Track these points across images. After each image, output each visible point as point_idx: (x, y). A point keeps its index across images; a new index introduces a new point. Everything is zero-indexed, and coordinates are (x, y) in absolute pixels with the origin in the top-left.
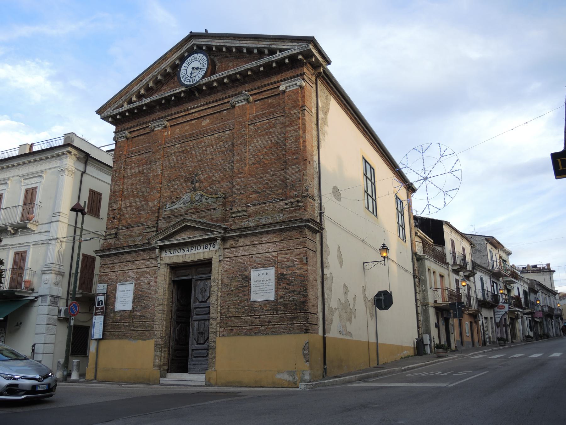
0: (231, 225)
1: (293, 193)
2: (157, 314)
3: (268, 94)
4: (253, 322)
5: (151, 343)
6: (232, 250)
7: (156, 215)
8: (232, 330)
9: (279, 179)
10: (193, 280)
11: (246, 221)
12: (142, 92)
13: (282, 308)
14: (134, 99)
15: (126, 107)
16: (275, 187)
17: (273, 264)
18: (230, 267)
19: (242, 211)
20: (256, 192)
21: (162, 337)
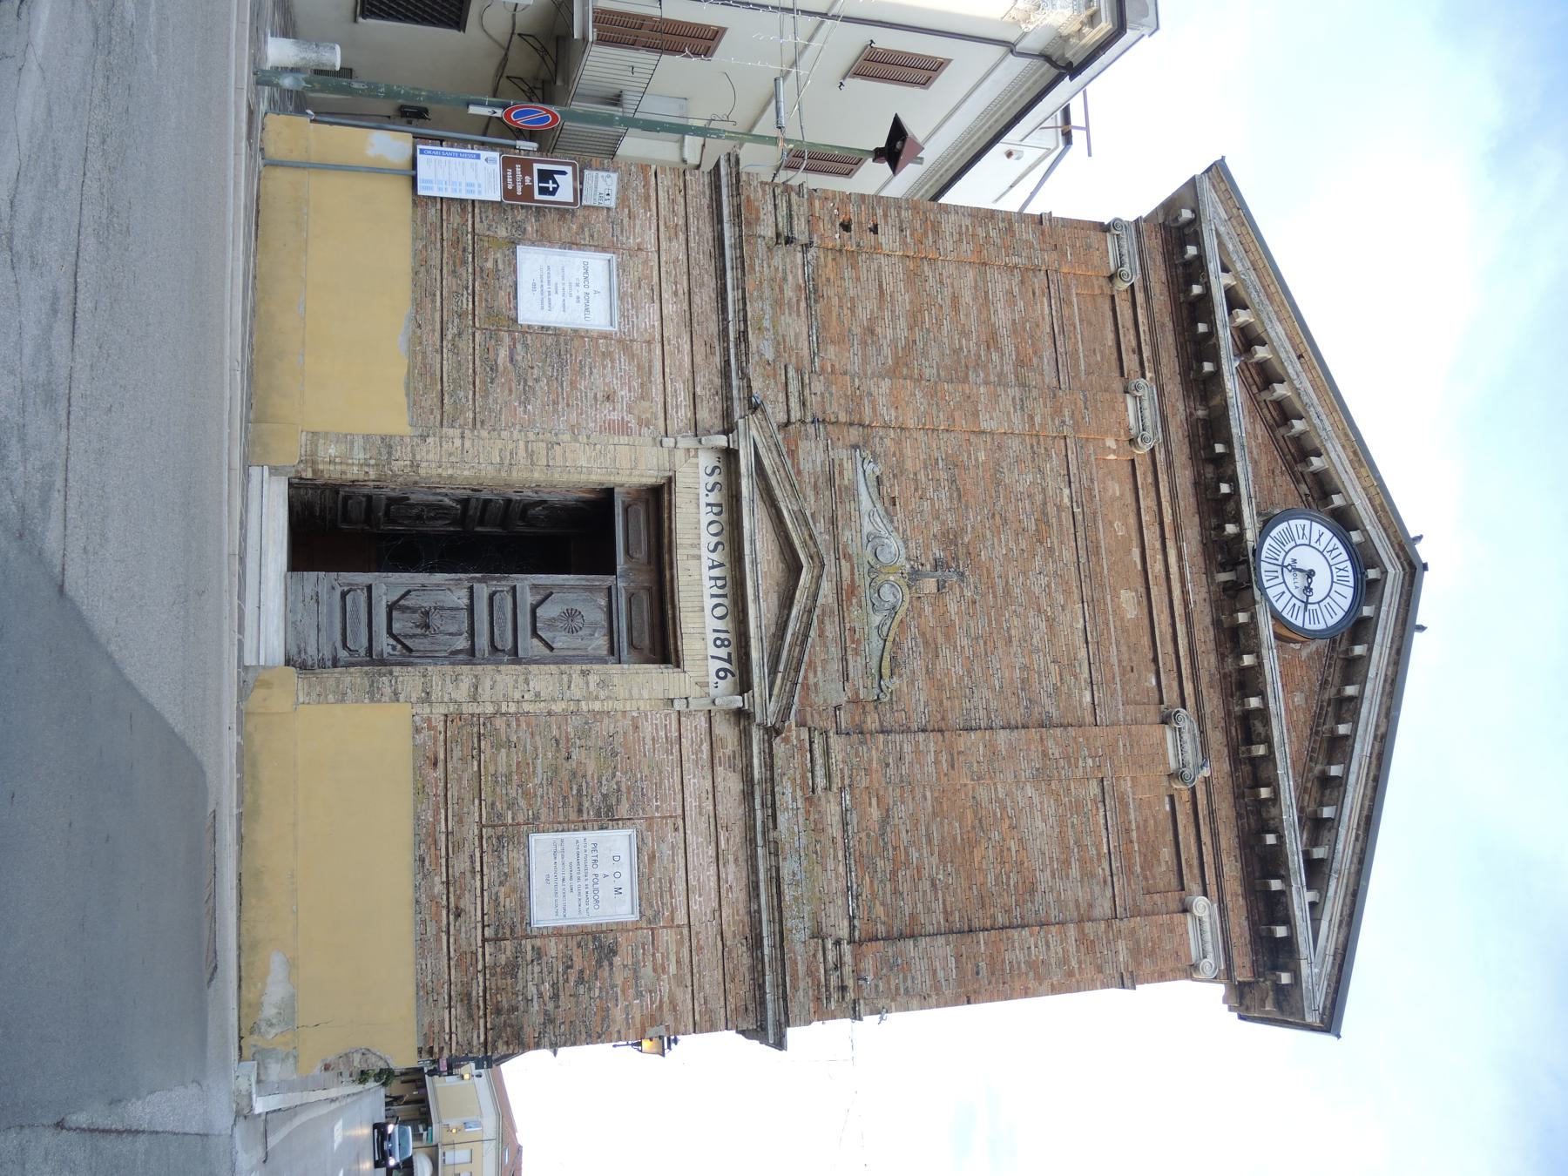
0: (786, 740)
1: (868, 965)
2: (499, 443)
3: (1188, 846)
4: (459, 847)
5: (394, 419)
6: (705, 747)
7: (843, 417)
8: (435, 764)
9: (920, 906)
10: (608, 580)
11: (794, 800)
12: (1261, 353)
13: (503, 959)
14: (1243, 317)
15: (1219, 282)
16: (895, 892)
17: (650, 913)
18: (649, 742)
19: (828, 776)
20: (885, 820)
21: (415, 466)
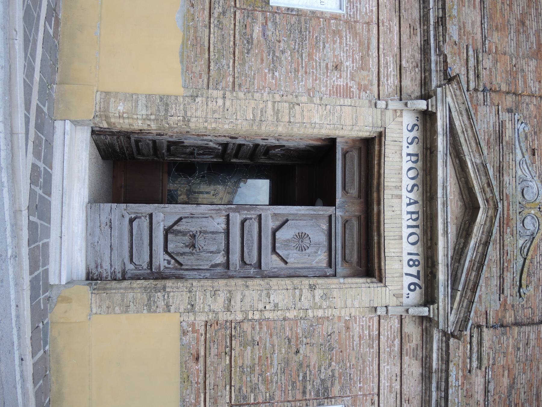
5: (168, 80)
6: (397, 342)
7: (504, 88)
8: (197, 359)
10: (330, 210)
18: (356, 339)
20: (511, 386)
21: (186, 120)
